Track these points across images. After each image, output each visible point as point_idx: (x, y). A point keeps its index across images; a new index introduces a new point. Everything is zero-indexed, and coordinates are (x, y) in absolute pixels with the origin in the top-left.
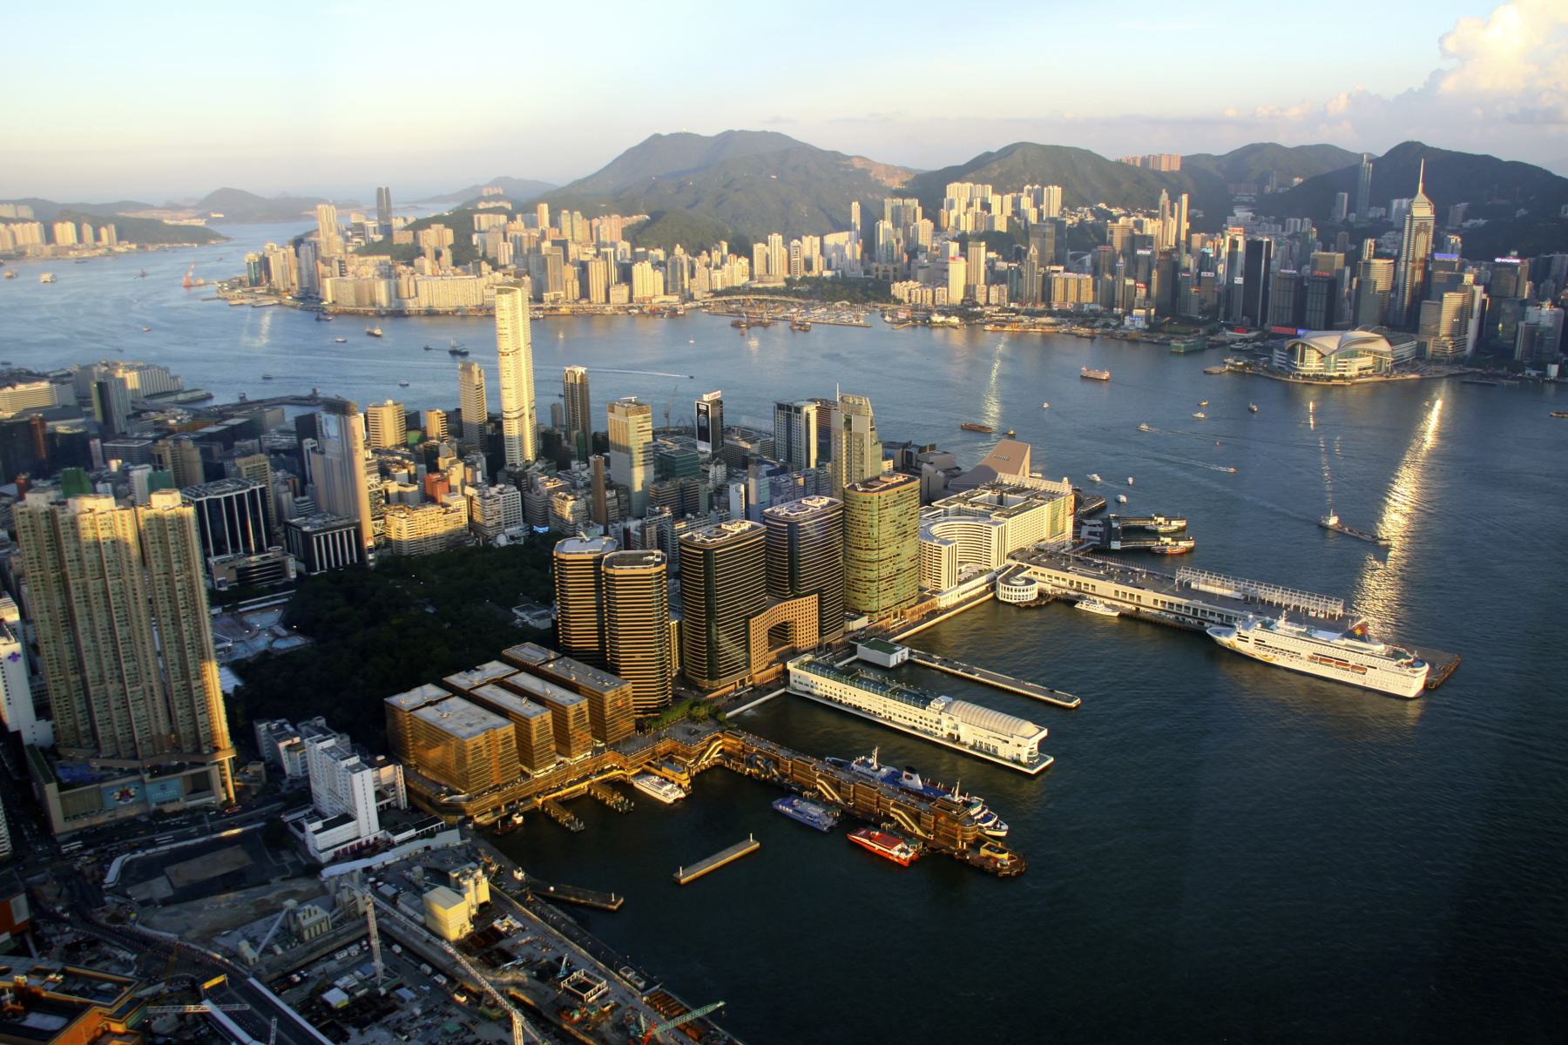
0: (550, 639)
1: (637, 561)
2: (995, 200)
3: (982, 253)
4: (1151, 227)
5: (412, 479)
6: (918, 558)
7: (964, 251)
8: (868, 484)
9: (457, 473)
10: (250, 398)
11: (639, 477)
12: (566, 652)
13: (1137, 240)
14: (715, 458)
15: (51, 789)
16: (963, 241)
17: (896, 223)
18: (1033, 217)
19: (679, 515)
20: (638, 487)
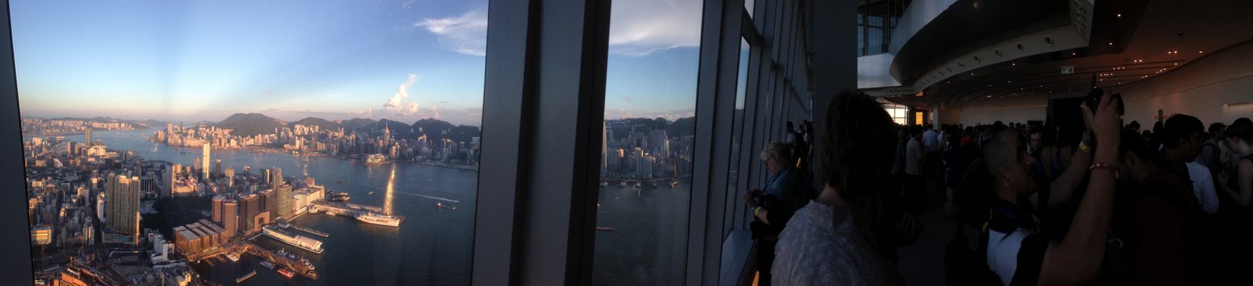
0: (210, 219)
1: (230, 202)
2: (305, 128)
3: (303, 139)
4: (336, 134)
5: (183, 180)
6: (291, 203)
7: (299, 139)
8: (281, 187)
9: (192, 180)
10: (152, 160)
11: (231, 183)
12: (213, 222)
13: (334, 137)
14: (247, 180)
15: (103, 233)
16: (299, 137)
17: (285, 131)
18: (313, 131)
19: (239, 193)
20: (230, 185)
